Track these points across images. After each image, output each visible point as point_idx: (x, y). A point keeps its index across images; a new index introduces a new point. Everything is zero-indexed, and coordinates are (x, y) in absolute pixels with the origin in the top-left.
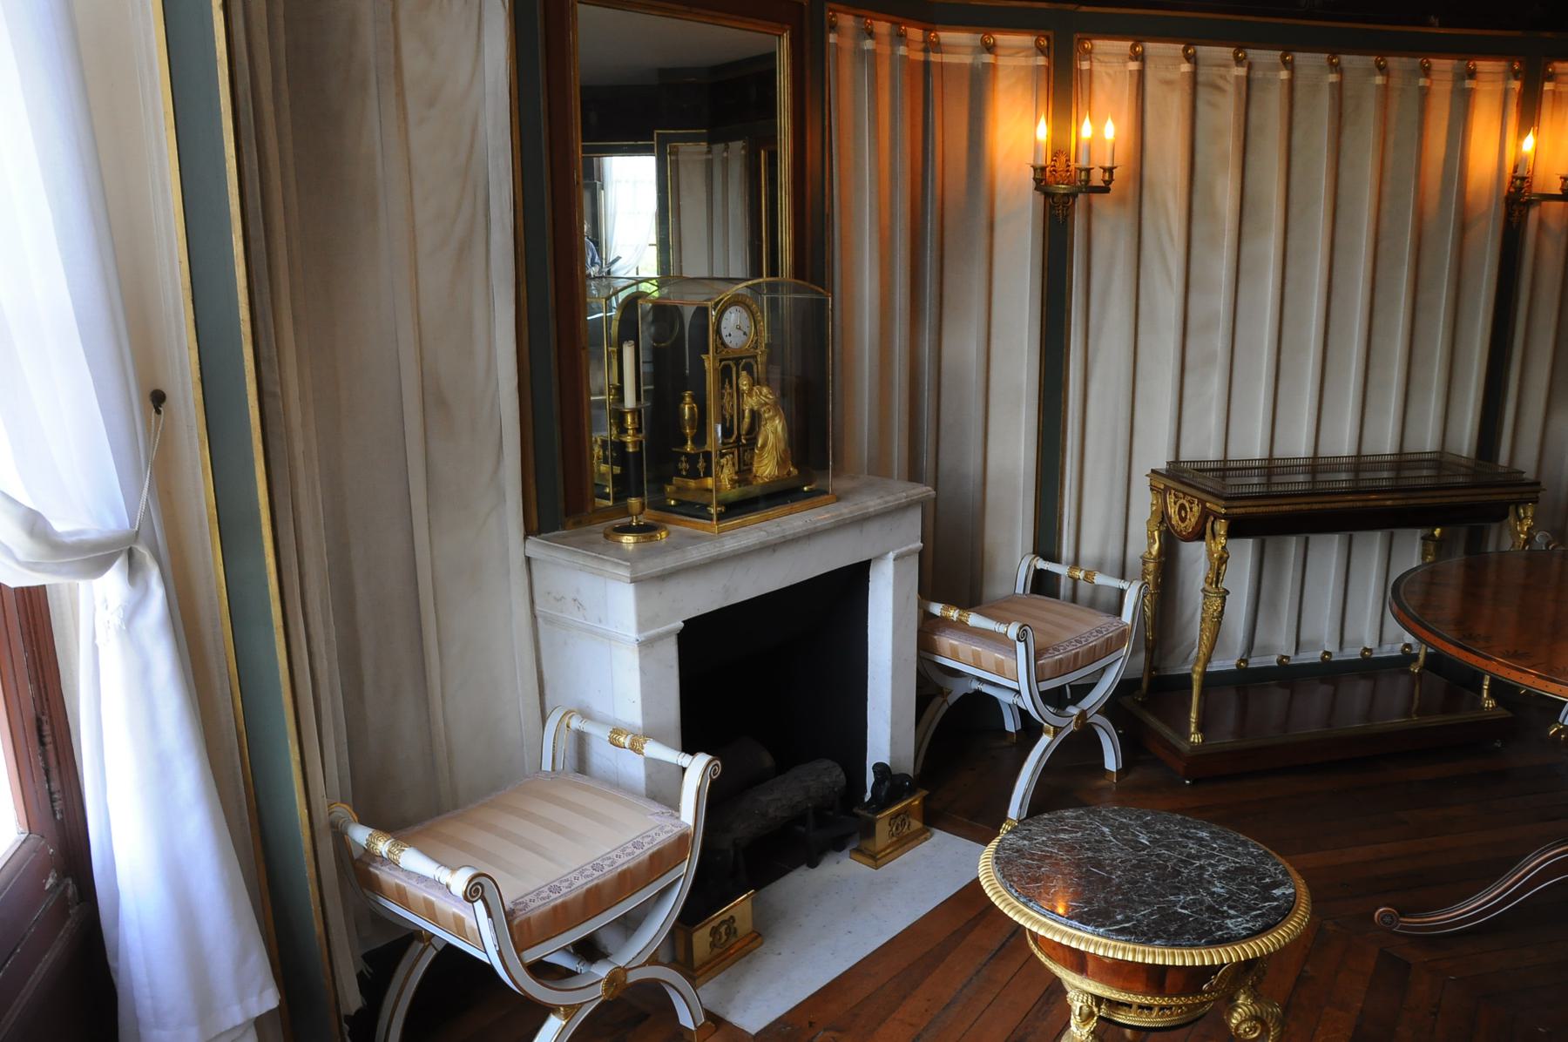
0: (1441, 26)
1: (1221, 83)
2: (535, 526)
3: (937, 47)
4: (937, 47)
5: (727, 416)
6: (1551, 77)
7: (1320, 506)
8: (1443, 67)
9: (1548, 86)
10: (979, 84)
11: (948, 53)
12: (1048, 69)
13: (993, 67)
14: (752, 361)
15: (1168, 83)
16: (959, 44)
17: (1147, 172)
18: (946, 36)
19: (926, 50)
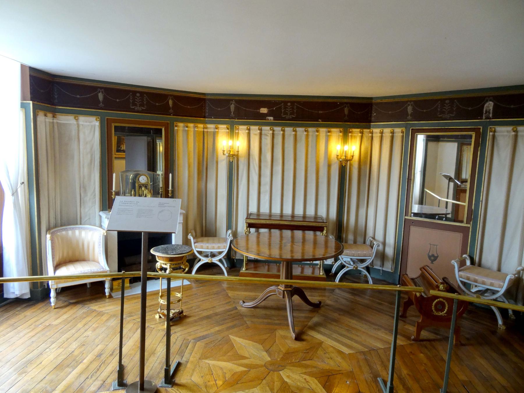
0: (322, 121)
1: (268, 134)
2: (102, 210)
3: (207, 128)
4: (207, 128)
5: (141, 195)
6: (350, 132)
7: (268, 222)
8: (323, 130)
9: (350, 134)
10: (214, 135)
11: (209, 129)
12: (229, 132)
14: (147, 185)
16: (211, 127)
17: (251, 152)
18: (209, 126)
19: (204, 129)
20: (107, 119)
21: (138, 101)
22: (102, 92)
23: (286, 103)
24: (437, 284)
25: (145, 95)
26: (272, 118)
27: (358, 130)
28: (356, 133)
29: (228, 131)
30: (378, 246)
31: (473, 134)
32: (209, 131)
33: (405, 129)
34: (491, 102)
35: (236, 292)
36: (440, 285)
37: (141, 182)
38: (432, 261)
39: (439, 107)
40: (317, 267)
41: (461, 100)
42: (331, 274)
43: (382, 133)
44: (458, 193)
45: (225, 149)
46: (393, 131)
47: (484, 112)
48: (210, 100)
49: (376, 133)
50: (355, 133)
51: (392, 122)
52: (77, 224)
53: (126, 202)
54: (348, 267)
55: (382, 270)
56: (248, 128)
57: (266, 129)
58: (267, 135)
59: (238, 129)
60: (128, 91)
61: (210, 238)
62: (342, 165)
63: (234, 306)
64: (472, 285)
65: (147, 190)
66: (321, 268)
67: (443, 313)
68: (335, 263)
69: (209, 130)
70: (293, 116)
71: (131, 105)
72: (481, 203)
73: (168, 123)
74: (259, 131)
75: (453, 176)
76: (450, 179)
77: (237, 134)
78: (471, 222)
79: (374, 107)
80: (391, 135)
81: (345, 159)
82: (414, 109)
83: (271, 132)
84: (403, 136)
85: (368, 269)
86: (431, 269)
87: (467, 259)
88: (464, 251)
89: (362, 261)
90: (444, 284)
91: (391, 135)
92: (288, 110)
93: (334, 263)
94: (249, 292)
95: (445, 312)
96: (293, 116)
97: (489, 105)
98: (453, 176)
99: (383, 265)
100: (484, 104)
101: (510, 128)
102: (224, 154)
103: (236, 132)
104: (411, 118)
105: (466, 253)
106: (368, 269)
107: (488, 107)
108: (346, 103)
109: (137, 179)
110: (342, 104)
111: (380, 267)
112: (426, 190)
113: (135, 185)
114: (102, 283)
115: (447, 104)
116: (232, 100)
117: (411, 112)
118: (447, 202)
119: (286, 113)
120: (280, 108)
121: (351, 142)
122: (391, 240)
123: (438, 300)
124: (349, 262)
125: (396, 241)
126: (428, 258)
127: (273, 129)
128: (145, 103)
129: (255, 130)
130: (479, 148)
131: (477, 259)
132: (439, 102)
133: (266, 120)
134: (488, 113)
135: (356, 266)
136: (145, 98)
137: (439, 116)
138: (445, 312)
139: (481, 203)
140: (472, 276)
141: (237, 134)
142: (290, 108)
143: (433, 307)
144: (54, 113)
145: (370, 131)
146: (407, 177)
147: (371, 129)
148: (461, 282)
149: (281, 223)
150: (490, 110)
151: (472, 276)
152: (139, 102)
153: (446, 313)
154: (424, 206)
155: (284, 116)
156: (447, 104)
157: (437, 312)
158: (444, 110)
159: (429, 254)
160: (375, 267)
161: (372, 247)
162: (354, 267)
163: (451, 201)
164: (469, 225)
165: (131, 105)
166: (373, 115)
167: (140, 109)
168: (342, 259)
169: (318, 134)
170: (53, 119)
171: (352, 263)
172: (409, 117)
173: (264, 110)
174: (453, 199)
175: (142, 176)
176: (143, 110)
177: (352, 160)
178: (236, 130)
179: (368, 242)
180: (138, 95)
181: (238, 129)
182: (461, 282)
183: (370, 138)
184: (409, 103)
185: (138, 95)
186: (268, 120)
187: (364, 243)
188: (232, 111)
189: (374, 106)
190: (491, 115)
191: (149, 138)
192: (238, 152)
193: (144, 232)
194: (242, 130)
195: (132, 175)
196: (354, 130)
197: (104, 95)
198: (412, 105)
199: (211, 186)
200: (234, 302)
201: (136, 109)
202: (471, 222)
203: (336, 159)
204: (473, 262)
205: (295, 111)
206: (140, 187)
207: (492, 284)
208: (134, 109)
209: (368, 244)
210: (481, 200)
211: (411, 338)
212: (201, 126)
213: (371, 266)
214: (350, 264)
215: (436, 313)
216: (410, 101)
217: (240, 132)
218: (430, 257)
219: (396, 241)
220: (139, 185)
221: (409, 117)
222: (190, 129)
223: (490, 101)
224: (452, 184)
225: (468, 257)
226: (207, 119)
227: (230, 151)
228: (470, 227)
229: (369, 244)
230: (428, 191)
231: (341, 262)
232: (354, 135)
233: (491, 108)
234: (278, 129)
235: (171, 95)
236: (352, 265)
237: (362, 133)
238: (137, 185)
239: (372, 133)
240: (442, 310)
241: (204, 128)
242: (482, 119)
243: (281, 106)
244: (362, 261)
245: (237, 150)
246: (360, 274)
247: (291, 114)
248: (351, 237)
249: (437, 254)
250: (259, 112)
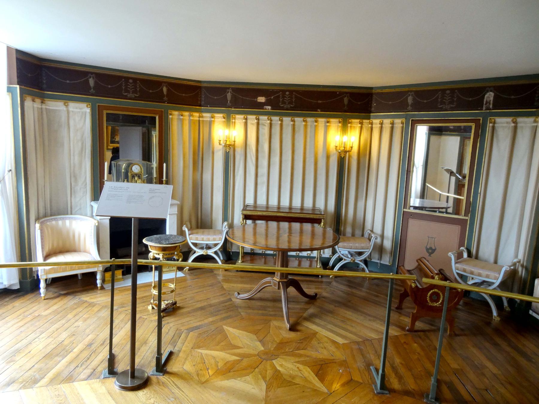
0: (321, 111)
1: (265, 124)
3: (202, 117)
4: (202, 117)
6: (349, 123)
8: (322, 121)
9: (349, 125)
10: (210, 124)
12: (225, 121)
13: (214, 121)
15: (252, 124)
17: (248, 143)
18: (205, 115)
19: (199, 118)
20: (99, 106)
21: (131, 88)
22: (93, 78)
23: (284, 92)
24: (432, 275)
25: (138, 82)
26: (270, 107)
27: (358, 121)
28: (355, 123)
29: (224, 120)
30: (376, 239)
31: (473, 125)
32: (205, 120)
33: (405, 120)
34: (491, 93)
35: (232, 285)
36: (435, 276)
37: (134, 171)
38: (430, 254)
39: (440, 97)
40: (314, 260)
41: (461, 90)
42: (328, 267)
43: (382, 124)
44: (459, 189)
45: (221, 139)
46: (393, 122)
47: (485, 103)
48: (205, 87)
49: (376, 124)
50: (355, 124)
51: (392, 112)
52: (67, 214)
53: (115, 188)
54: (345, 260)
55: (380, 263)
56: (246, 117)
57: (264, 119)
58: (264, 125)
59: (235, 118)
60: (119, 78)
61: (206, 231)
62: (341, 157)
63: (228, 297)
64: (468, 278)
65: (140, 180)
66: (319, 261)
67: (438, 304)
68: (333, 256)
69: (204, 119)
70: (291, 106)
71: (123, 91)
72: (479, 195)
73: (162, 111)
74: (256, 121)
75: (455, 170)
76: (451, 173)
77: (233, 123)
78: (469, 215)
79: (374, 97)
80: (390, 125)
81: (344, 150)
82: (414, 99)
83: (269, 122)
84: (403, 127)
85: (365, 262)
86: (428, 261)
87: (465, 252)
88: (461, 244)
89: (360, 254)
90: (439, 275)
91: (390, 125)
92: (286, 100)
93: (331, 256)
94: (244, 284)
95: (439, 302)
96: (291, 106)
98: (454, 170)
99: (380, 258)
100: (484, 95)
101: (509, 119)
102: (220, 144)
103: (232, 122)
104: (411, 108)
105: (464, 246)
106: (365, 262)
107: (488, 97)
108: (346, 93)
109: (130, 168)
110: (341, 93)
111: (378, 260)
112: (427, 184)
113: (128, 175)
114: (93, 275)
116: (229, 88)
118: (448, 197)
119: (284, 103)
120: (278, 97)
121: (350, 133)
122: (389, 233)
123: (433, 290)
124: (347, 255)
125: (395, 234)
126: (425, 250)
127: (270, 118)
128: (138, 90)
129: (252, 119)
131: (474, 251)
132: (440, 92)
133: (263, 109)
134: (488, 104)
135: (353, 259)
136: (138, 85)
138: (439, 302)
139: (479, 195)
140: (468, 268)
141: (233, 123)
142: (289, 97)
143: (428, 298)
144: (43, 98)
145: (370, 122)
146: (406, 169)
147: (371, 120)
148: (458, 274)
149: (278, 215)
150: (490, 101)
151: (468, 268)
152: (132, 89)
153: (440, 304)
154: (425, 200)
155: (283, 105)
157: (432, 303)
159: (426, 247)
160: (373, 260)
161: (370, 240)
162: (352, 260)
163: (452, 195)
164: (467, 218)
165: (123, 91)
167: (133, 96)
168: (340, 252)
169: (316, 124)
170: (42, 105)
171: (349, 256)
172: (409, 108)
173: (262, 99)
174: (455, 194)
175: (135, 166)
176: (136, 97)
177: (351, 151)
178: (232, 119)
179: (366, 235)
180: (131, 81)
181: (235, 119)
182: (458, 274)
183: (370, 129)
184: (409, 93)
185: (131, 81)
186: (266, 109)
187: (363, 235)
188: (228, 99)
189: (374, 95)
190: (491, 106)
191: (144, 129)
192: (235, 141)
193: (134, 218)
194: (239, 119)
195: (124, 165)
196: (354, 121)
197: (94, 80)
198: (412, 95)
199: (207, 176)
200: (229, 294)
201: (129, 96)
202: (469, 215)
203: (335, 150)
204: (470, 255)
205: (294, 100)
206: (133, 177)
207: (487, 276)
208: (126, 96)
209: (366, 237)
210: (479, 192)
211: (406, 328)
212: (196, 114)
213: (369, 259)
214: (348, 257)
215: (430, 304)
216: (411, 91)
217: (236, 121)
218: (427, 250)
219: (395, 234)
220: (132, 174)
221: (409, 107)
222: (185, 118)
223: (491, 91)
224: (453, 179)
225: (465, 250)
226: (202, 108)
227: (226, 141)
228: (467, 220)
229: (367, 237)
230: (429, 185)
231: (338, 255)
232: (354, 125)
233: (492, 99)
234: (275, 119)
235: (165, 82)
236: (350, 258)
237: (361, 123)
238: (129, 174)
239: (372, 124)
240: (437, 301)
241: (199, 117)
242: (482, 110)
243: (279, 95)
244: (360, 254)
245: (234, 140)
246: (358, 267)
247: (290, 103)
248: (349, 230)
249: (435, 247)
250: (257, 101)
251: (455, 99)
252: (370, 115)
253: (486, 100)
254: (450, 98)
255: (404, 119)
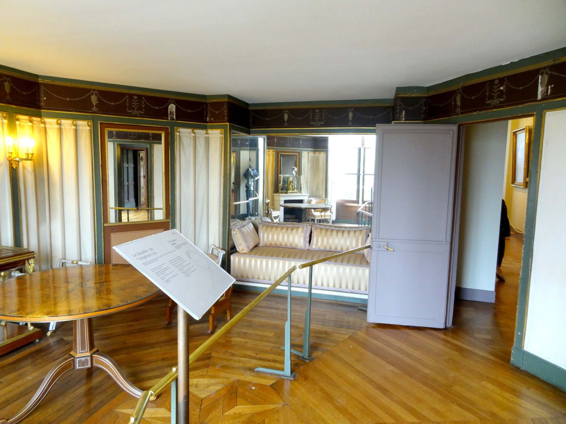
6: (18, 120)
9: (17, 123)
27: (27, 117)
33: (92, 122)
34: (173, 105)
41: (148, 98)
47: (169, 113)
79: (42, 88)
82: (99, 100)
84: (91, 130)
97: (172, 108)
104: (97, 109)
107: (171, 108)
108: (8, 76)
115: (136, 100)
117: (96, 103)
130: (170, 147)
132: (127, 96)
134: (172, 115)
137: (129, 111)
156: (136, 100)
158: (133, 106)
166: (43, 100)
190: (175, 117)
198: (96, 94)
216: (94, 90)
223: (173, 103)
232: (22, 124)
233: (174, 110)
251: (143, 106)
252: (41, 112)
253: (170, 111)
254: (138, 104)
255: (91, 121)
